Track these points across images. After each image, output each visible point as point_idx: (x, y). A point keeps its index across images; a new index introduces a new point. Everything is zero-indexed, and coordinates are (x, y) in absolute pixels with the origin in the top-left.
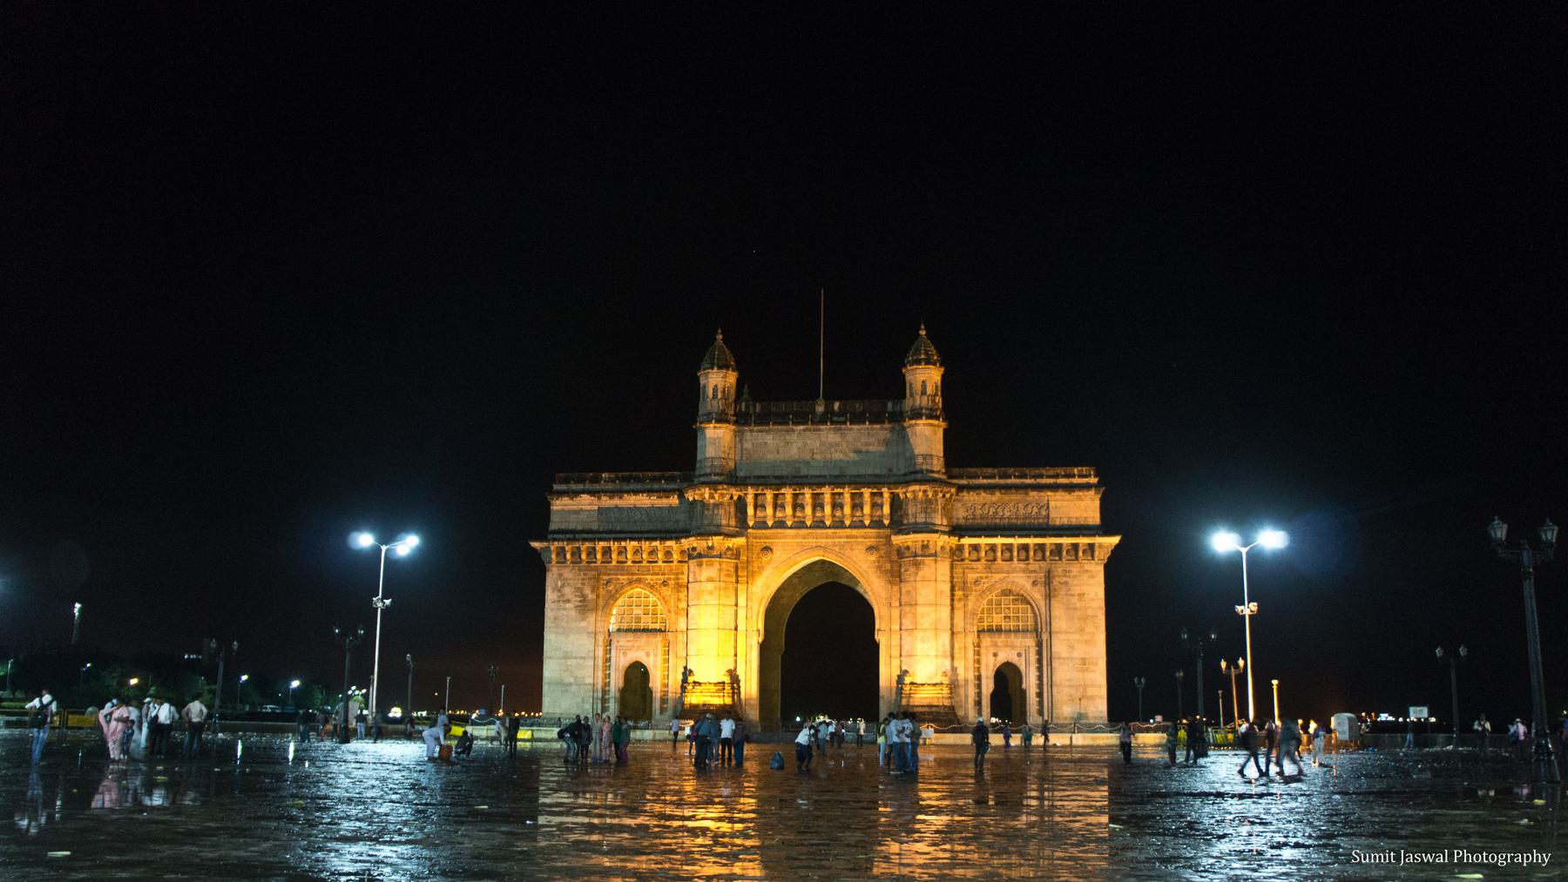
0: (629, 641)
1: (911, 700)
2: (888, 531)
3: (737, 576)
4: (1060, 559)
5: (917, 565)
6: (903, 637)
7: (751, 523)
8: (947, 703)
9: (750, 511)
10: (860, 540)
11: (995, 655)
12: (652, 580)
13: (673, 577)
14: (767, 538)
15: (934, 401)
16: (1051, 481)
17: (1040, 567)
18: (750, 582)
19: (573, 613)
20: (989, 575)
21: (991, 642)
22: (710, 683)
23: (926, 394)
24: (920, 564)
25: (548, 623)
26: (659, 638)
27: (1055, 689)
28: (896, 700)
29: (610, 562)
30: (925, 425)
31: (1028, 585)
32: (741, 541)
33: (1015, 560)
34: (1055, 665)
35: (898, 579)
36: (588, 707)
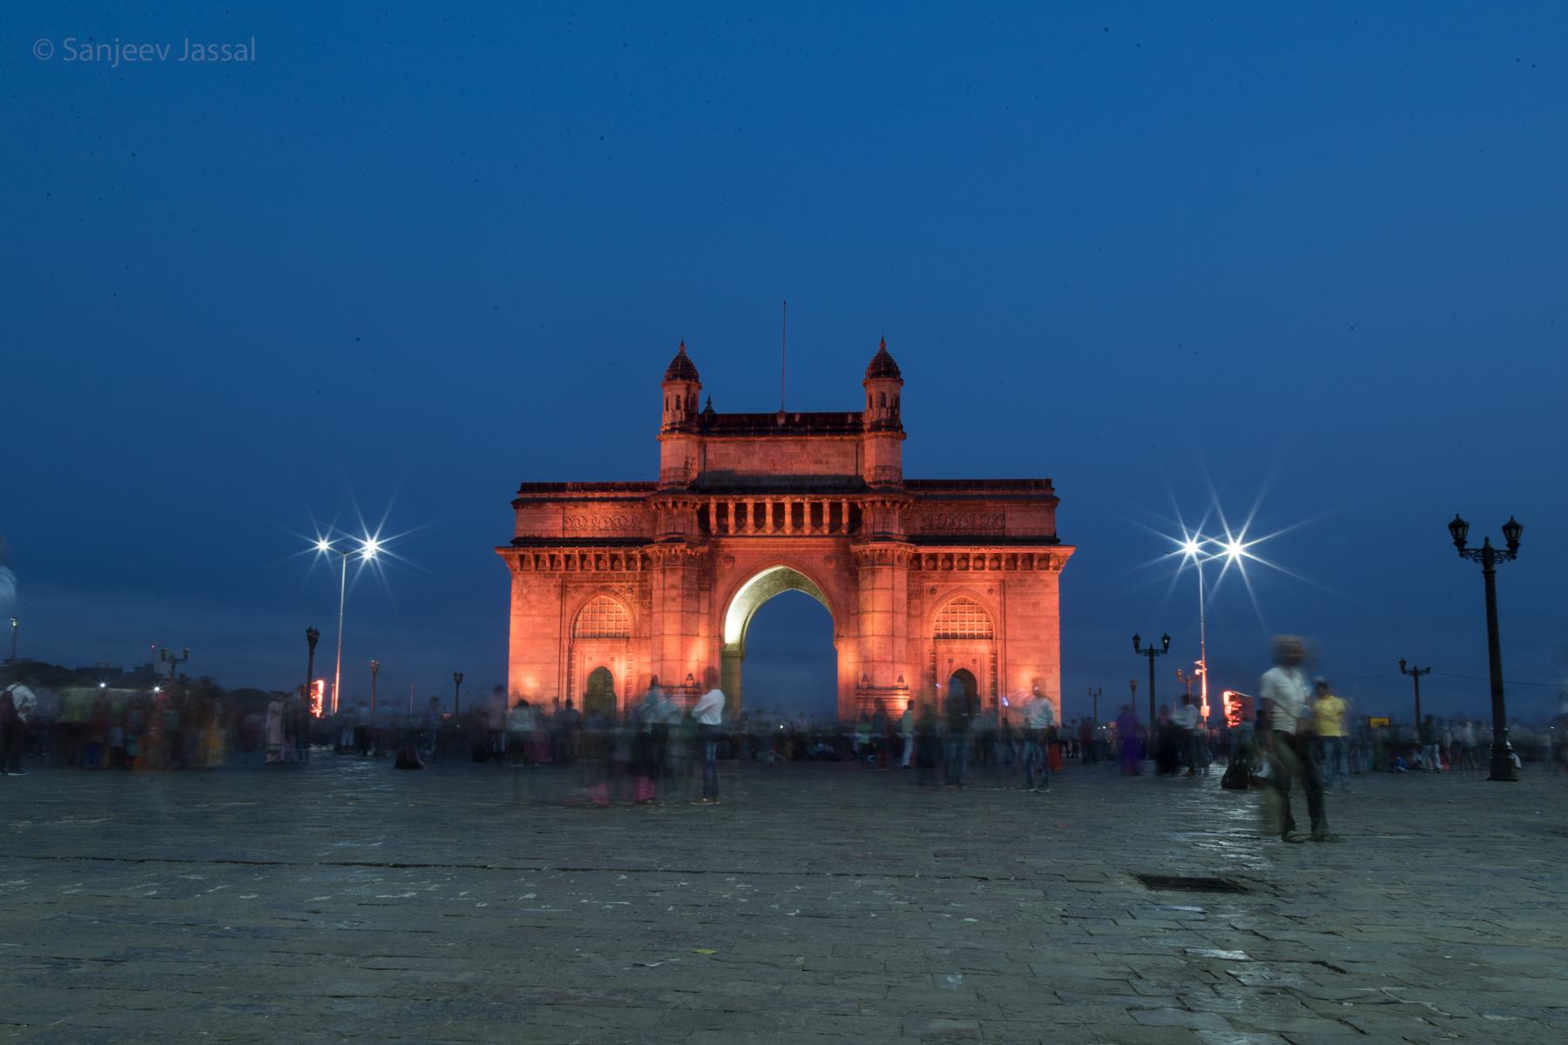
4: (1016, 569)
5: (873, 573)
7: (714, 532)
9: (713, 519)
10: (819, 549)
13: (637, 584)
14: (729, 546)
19: (538, 619)
20: (946, 584)
23: (885, 406)
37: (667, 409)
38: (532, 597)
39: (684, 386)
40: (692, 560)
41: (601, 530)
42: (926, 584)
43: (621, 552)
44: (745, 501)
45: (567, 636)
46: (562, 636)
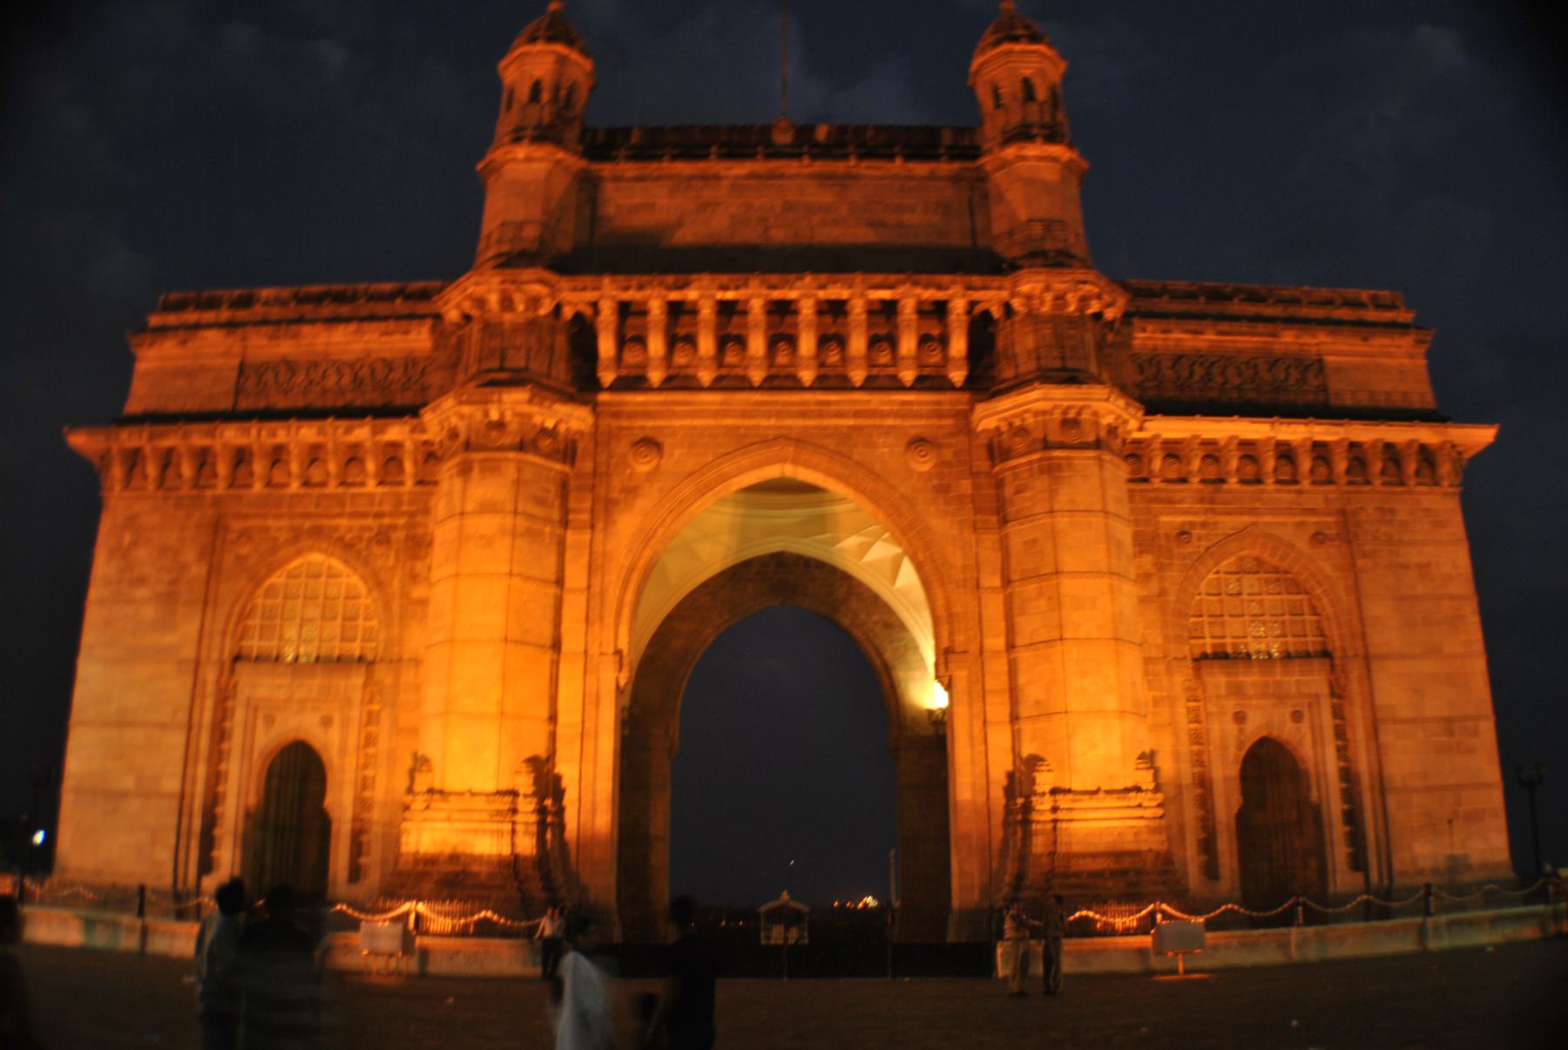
0: (280, 687)
1: (1062, 839)
2: (965, 397)
3: (565, 511)
6: (1022, 666)
7: (607, 377)
8: (1155, 843)
9: (606, 346)
10: (890, 422)
11: (1240, 718)
12: (349, 530)
13: (402, 521)
14: (648, 415)
15: (1053, 117)
16: (1319, 313)
17: (1326, 500)
18: (600, 526)
19: (149, 612)
20: (1211, 519)
21: (1229, 684)
22: (473, 794)
24: (1059, 468)
25: (91, 635)
26: (357, 679)
27: (1392, 801)
28: (1005, 843)
29: (250, 486)
30: (1040, 159)
31: (1302, 542)
32: (574, 418)
33: (1270, 480)
34: (1387, 737)
35: (994, 518)
36: (164, 855)
37: (509, 107)
38: (142, 553)
39: (551, 59)
40: (546, 443)
41: (325, 391)
42: (1165, 519)
43: (362, 432)
44: (692, 294)
45: (215, 655)
46: (204, 653)
